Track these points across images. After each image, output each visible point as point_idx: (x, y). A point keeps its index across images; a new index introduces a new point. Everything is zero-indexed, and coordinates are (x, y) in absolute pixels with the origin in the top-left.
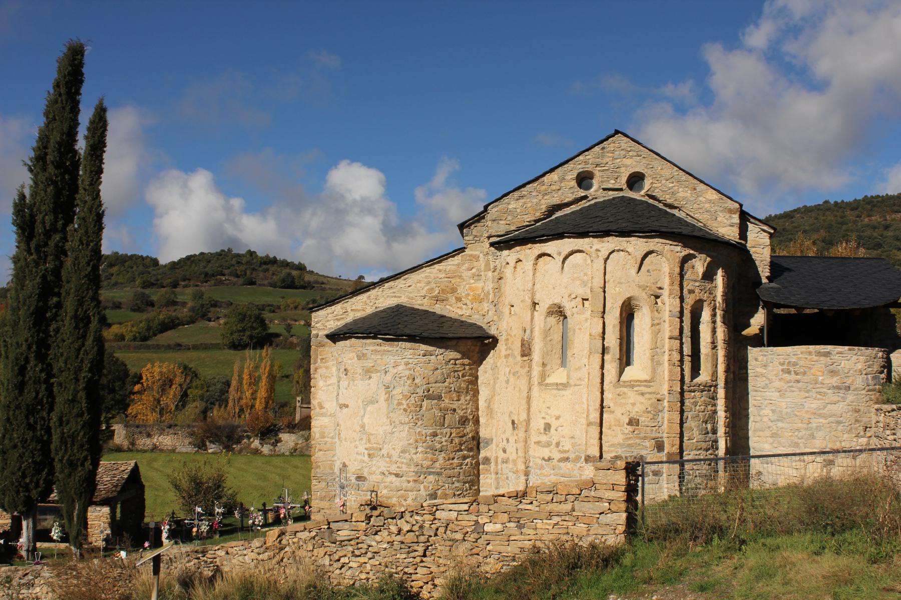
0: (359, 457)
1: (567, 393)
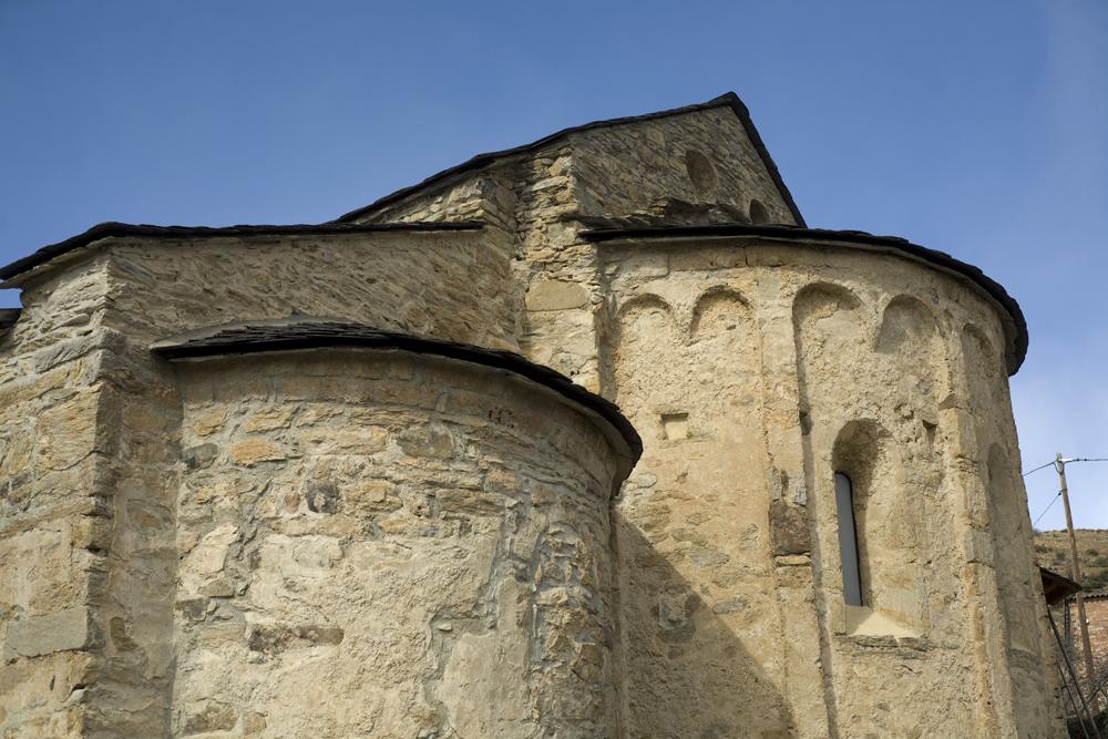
1: (928, 671)
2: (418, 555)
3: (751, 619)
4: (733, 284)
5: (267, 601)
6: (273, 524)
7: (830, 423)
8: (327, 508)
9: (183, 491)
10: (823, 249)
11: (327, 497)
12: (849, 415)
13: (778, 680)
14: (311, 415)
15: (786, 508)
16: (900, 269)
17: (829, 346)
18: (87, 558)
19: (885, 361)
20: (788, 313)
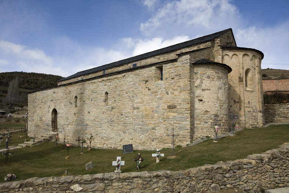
0: (216, 108)
1: (253, 94)
2: (217, 83)
3: (236, 88)
4: (236, 54)
5: (204, 86)
6: (204, 80)
7: (245, 68)
8: (209, 78)
9: (195, 76)
10: (246, 50)
11: (209, 77)
12: (247, 68)
13: (239, 94)
14: (207, 70)
15: (241, 77)
16: (253, 52)
17: (246, 60)
18: (189, 82)
19: (251, 62)
20: (242, 57)
